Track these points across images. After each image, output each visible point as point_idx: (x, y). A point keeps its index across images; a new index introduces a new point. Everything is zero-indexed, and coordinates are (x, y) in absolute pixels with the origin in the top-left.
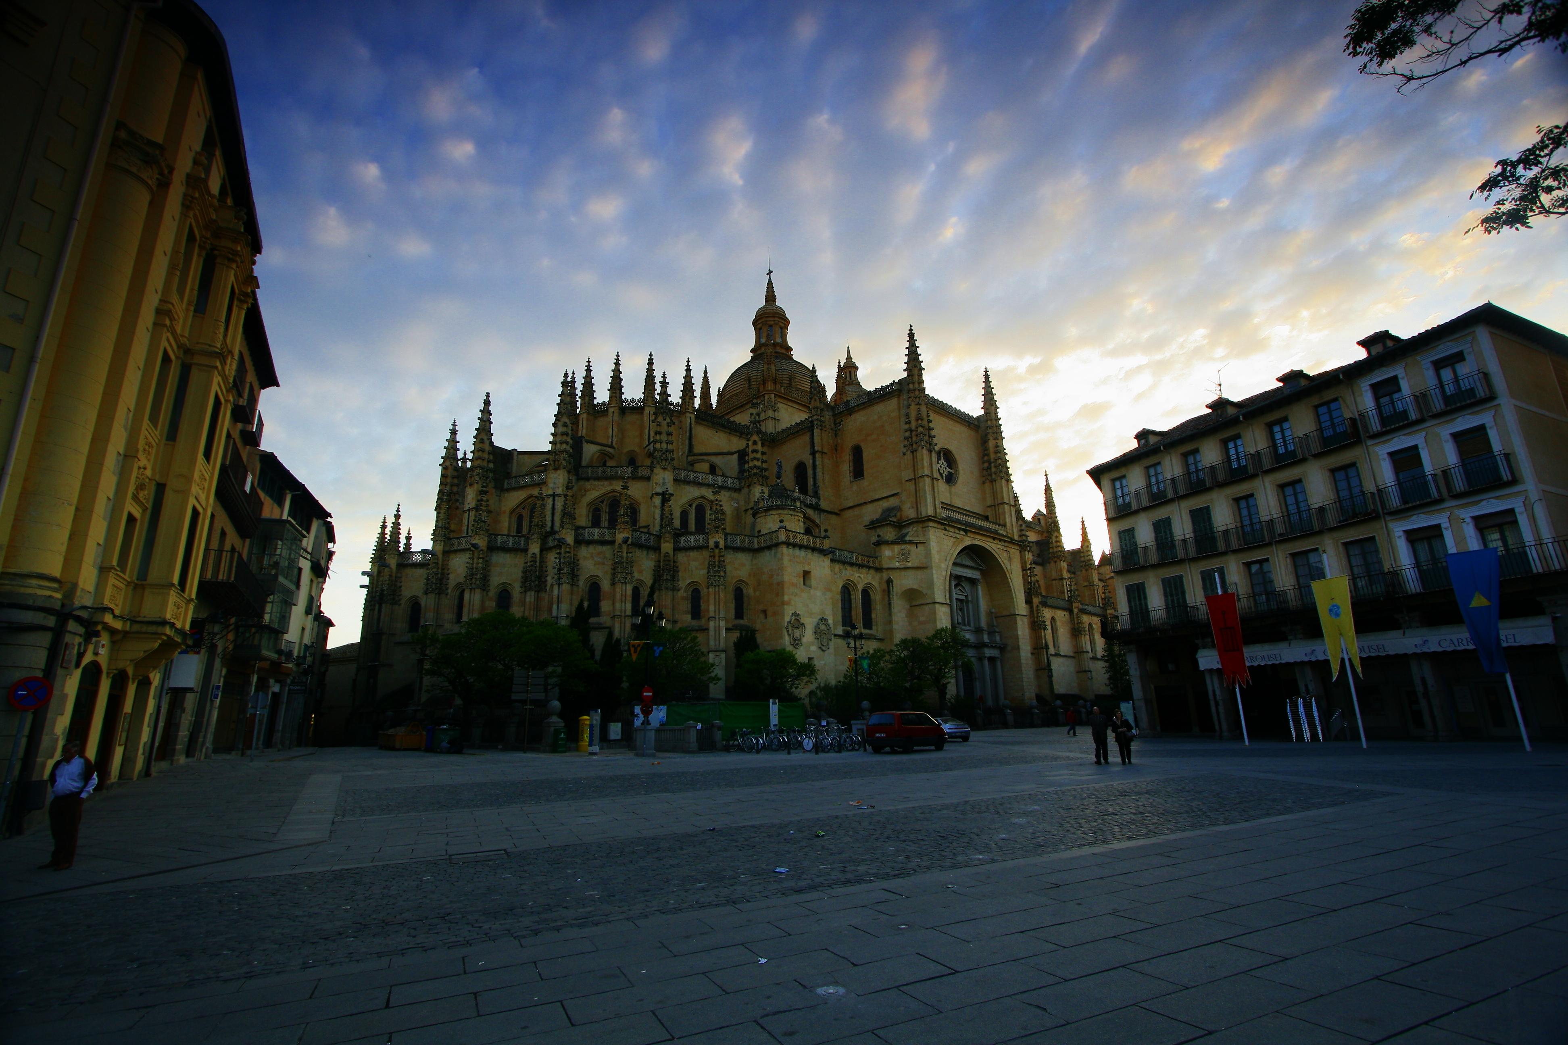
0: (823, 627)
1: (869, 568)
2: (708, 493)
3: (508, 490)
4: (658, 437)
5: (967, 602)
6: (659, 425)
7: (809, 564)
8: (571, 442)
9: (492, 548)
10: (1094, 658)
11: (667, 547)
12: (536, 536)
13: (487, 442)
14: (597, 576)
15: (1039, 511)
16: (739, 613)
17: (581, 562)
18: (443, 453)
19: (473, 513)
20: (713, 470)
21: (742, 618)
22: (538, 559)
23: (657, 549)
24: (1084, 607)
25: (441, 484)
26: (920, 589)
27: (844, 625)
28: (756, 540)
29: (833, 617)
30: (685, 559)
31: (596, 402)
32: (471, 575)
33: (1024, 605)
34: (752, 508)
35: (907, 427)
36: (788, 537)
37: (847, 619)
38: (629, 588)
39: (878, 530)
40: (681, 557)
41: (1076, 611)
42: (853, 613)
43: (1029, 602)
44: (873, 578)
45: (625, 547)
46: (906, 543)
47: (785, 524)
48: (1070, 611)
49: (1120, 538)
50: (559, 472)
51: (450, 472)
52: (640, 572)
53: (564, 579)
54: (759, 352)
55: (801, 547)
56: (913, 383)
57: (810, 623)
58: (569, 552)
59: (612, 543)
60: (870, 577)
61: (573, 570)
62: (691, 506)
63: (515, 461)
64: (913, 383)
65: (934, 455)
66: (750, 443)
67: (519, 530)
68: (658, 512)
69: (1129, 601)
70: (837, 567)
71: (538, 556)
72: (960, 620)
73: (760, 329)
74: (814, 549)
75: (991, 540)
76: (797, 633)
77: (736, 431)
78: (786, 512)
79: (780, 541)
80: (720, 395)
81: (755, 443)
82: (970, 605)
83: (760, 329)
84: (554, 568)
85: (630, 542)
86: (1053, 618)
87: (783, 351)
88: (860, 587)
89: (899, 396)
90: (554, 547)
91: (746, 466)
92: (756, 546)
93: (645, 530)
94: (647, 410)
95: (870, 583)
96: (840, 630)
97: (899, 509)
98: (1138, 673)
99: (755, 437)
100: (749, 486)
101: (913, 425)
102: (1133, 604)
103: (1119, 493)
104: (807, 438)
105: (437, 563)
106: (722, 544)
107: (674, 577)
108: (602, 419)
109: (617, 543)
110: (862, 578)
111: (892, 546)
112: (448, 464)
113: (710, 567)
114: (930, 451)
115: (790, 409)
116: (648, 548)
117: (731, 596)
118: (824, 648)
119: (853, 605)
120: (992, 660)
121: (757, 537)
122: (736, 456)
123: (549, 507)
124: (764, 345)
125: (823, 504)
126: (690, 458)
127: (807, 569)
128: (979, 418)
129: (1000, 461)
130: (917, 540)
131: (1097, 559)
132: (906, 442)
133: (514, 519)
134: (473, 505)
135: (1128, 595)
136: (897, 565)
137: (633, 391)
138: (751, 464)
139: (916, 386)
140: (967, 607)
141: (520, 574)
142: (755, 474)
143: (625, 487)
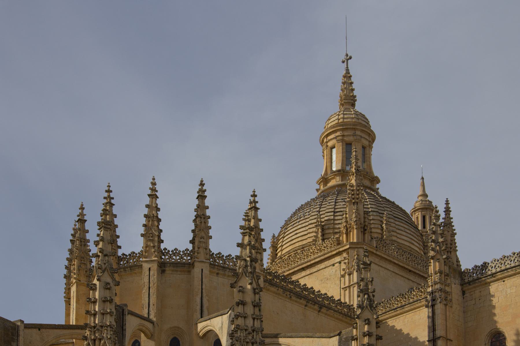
31: (120, 253)
54: (330, 184)
77: (315, 303)
87: (367, 183)
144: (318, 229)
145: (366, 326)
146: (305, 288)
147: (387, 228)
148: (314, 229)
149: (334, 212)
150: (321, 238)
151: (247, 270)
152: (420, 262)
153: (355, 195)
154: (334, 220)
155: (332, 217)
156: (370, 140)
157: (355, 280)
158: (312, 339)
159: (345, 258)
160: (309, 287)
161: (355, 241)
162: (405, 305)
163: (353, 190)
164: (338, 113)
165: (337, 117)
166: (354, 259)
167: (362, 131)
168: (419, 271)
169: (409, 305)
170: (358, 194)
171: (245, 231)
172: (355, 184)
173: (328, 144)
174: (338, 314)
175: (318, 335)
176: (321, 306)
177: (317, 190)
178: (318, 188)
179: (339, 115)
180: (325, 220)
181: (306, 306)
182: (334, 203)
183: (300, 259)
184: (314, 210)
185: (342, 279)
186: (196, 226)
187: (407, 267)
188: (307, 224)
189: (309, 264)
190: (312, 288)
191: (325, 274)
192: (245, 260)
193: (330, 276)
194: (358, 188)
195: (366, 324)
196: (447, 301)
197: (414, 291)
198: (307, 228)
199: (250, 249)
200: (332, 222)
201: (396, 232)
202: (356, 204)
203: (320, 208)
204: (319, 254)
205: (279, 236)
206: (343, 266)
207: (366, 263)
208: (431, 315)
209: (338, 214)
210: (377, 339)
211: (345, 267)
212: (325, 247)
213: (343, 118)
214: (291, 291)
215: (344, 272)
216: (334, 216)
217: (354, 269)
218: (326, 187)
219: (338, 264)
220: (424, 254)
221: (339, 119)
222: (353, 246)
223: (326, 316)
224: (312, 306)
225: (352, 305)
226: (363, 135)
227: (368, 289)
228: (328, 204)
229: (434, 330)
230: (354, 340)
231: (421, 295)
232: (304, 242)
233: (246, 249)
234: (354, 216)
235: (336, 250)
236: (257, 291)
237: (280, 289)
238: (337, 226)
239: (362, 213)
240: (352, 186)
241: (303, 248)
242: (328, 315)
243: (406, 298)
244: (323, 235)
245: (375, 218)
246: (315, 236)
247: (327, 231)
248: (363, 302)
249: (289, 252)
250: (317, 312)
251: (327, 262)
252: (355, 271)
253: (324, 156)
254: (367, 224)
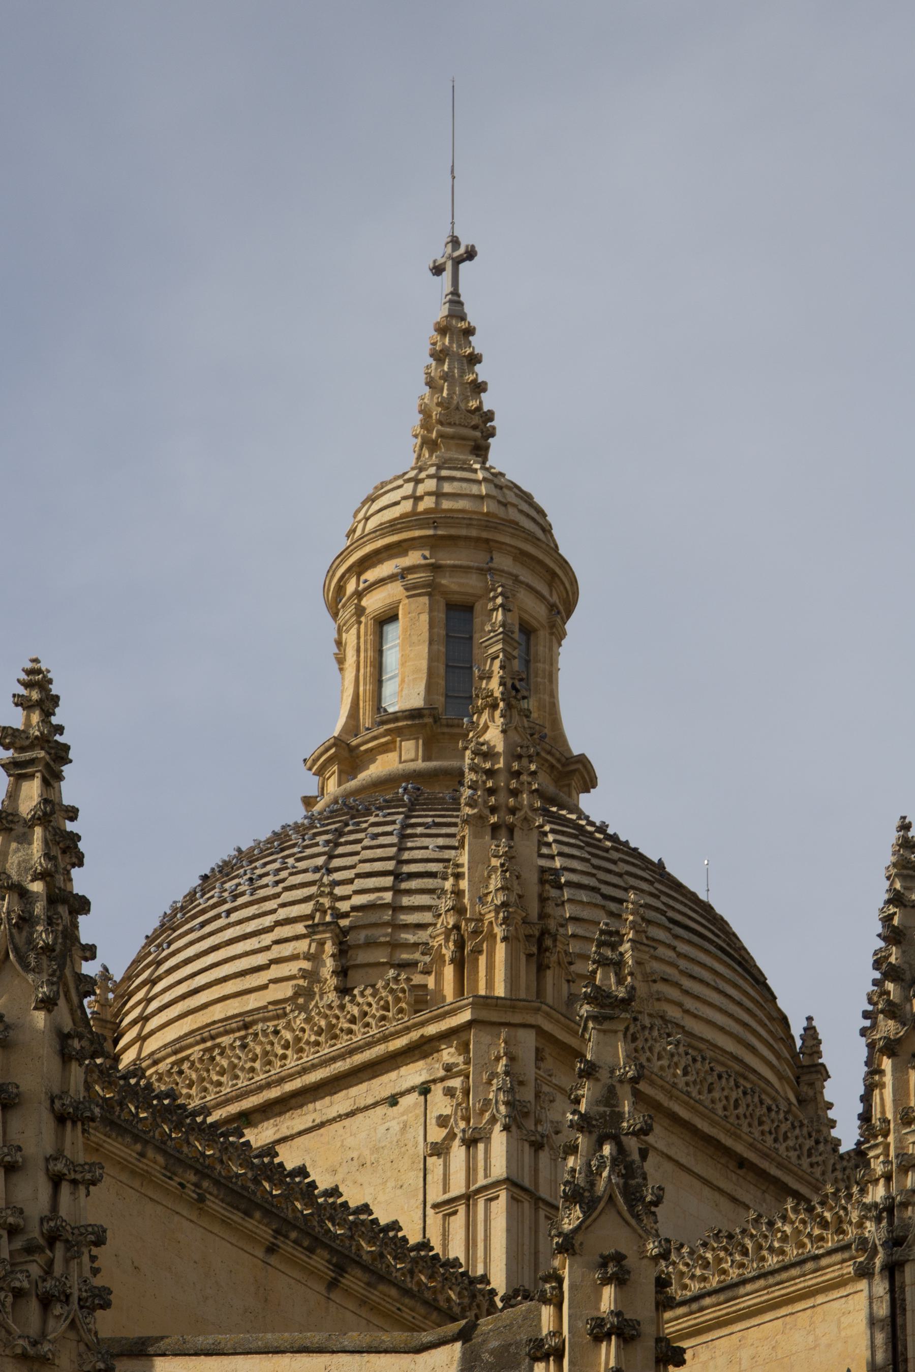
144: (322, 944)
145: (608, 1294)
146: (266, 1165)
147: (638, 963)
148: (302, 946)
149: (398, 876)
150: (332, 982)
151: (30, 941)
152: (784, 1127)
153: (502, 795)
154: (397, 908)
155: (388, 897)
156: (555, 599)
157: (499, 1169)
158: (325, 1359)
159: (448, 1068)
160: (289, 1166)
161: (500, 990)
162: (744, 1282)
163: (490, 773)
164: (412, 474)
165: (408, 488)
166: (494, 1075)
167: (522, 556)
168: (780, 1166)
169: (761, 1283)
170: (515, 793)
171: (27, 755)
172: (500, 748)
173: (364, 603)
174: (422, 1310)
175: (354, 1338)
176: (343, 1261)
177: (308, 802)
178: (314, 792)
179: (417, 481)
180: (354, 908)
181: (271, 1250)
182: (394, 839)
183: (232, 1071)
184: (302, 865)
185: (435, 1163)
187: (728, 1142)
188: (268, 921)
189: (274, 1093)
190: (302, 1171)
191: (350, 1141)
192: (23, 893)
193: (376, 1150)
194: (515, 766)
195: (606, 1281)
197: (784, 1218)
198: (267, 939)
199: (46, 842)
200: (387, 916)
201: (677, 985)
202: (504, 832)
203: (331, 857)
204: (325, 1050)
205: (129, 977)
206: (440, 1104)
207: (609, 995)
208: (883, 1310)
209: (414, 884)
210: (658, 1361)
211: (447, 1111)
212: (353, 1020)
213: (438, 495)
215: (444, 1132)
216: (398, 892)
217: (493, 1120)
218: (353, 784)
219: (414, 1097)
220: (800, 1102)
221: (417, 499)
222: (490, 1015)
223: (363, 1312)
224: (299, 1254)
225: (485, 1279)
226: (526, 576)
227: (620, 1116)
228: (367, 842)
230: (545, 1358)
231: (821, 1238)
232: (253, 1002)
233: (25, 839)
234: (495, 882)
235: (408, 1029)
236: (76, 1044)
237: (150, 1153)
238: (410, 937)
240: (489, 754)
241: (246, 1026)
242: (374, 1308)
243: (745, 1253)
244: (342, 972)
245: (585, 914)
246: (304, 974)
247: (362, 957)
248: (592, 1175)
249: (177, 1046)
250: (322, 1288)
251: (363, 1087)
252: (498, 1127)
253: (341, 661)
254: (552, 925)
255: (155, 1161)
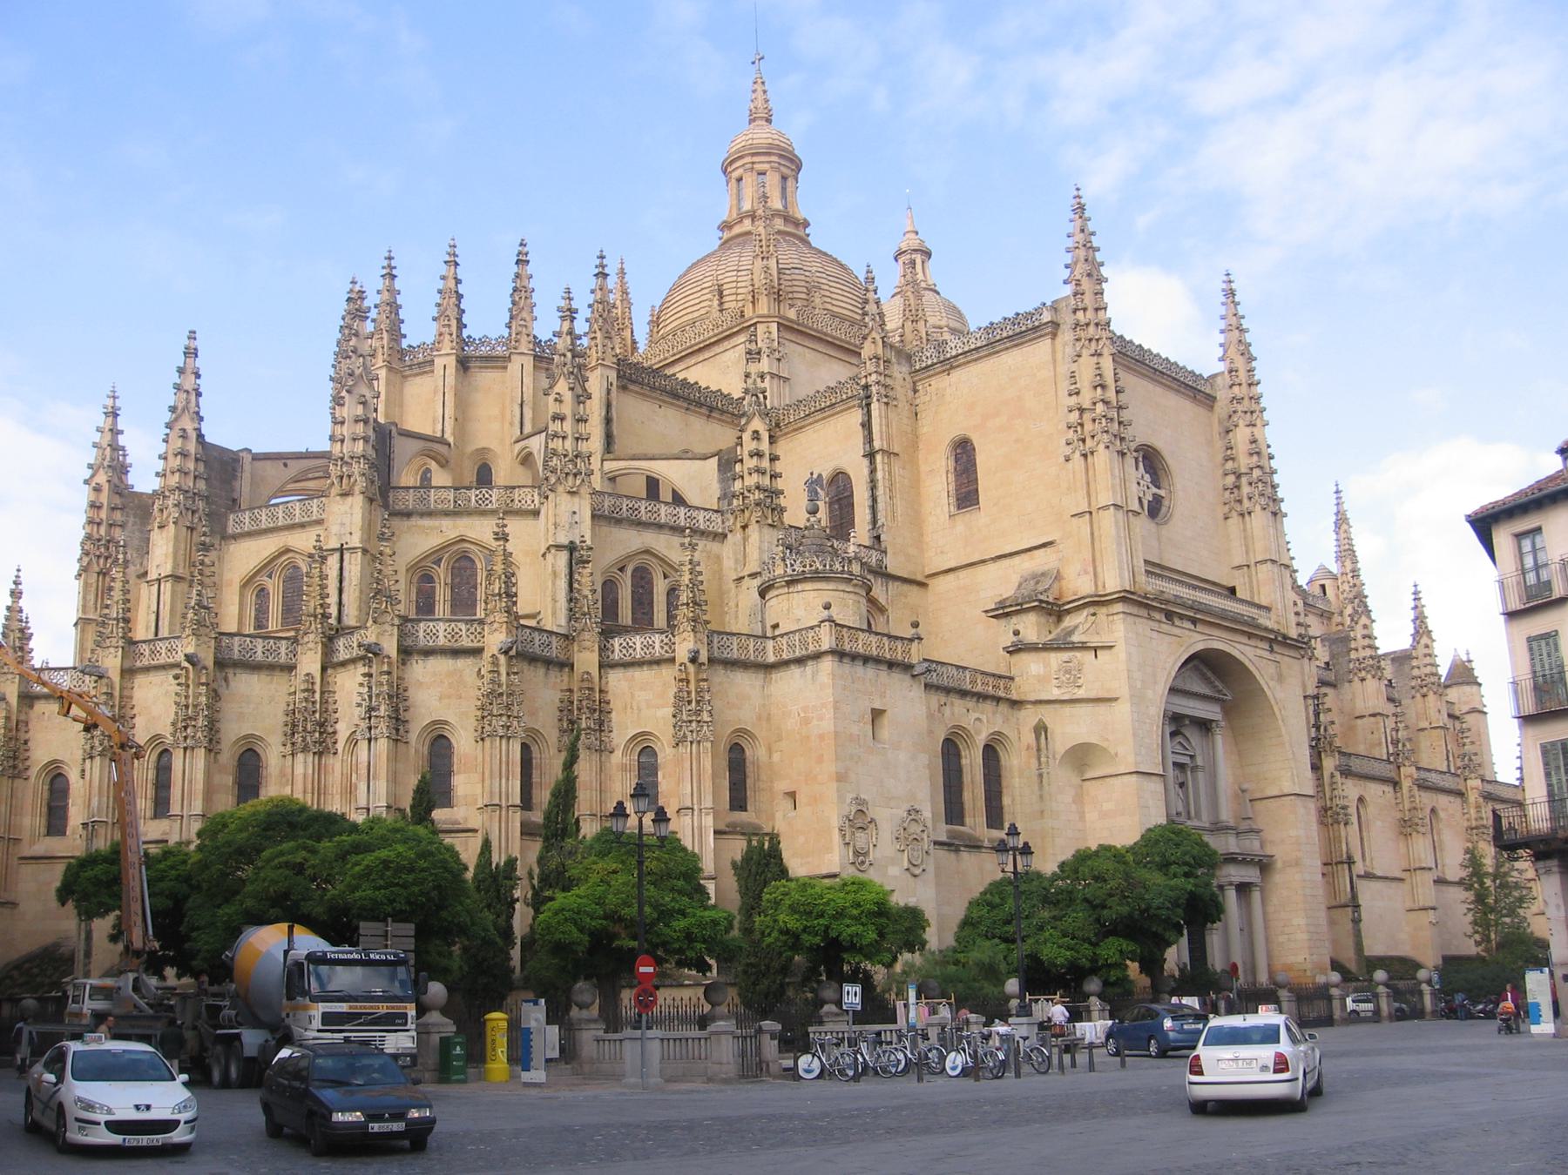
0: (915, 829)
1: (998, 700)
2: (669, 547)
3: (235, 537)
4: (555, 427)
5: (1195, 769)
6: (559, 400)
7: (883, 695)
8: (371, 433)
9: (220, 664)
10: (1440, 881)
11: (586, 659)
12: (312, 636)
13: (193, 435)
14: (446, 722)
15: (1322, 568)
16: (738, 800)
17: (410, 693)
18: (91, 456)
19: (167, 587)
20: (653, 485)
21: (743, 808)
22: (317, 687)
23: (566, 665)
24: (1424, 775)
25: (90, 522)
26: (1105, 744)
27: (949, 821)
28: (770, 644)
29: (929, 804)
30: (624, 684)
31: (405, 344)
32: (184, 723)
33: (1309, 773)
34: (753, 575)
35: (1073, 401)
36: (839, 639)
37: (954, 811)
38: (516, 748)
39: (1014, 619)
40: (617, 681)
41: (1406, 784)
42: (967, 796)
43: (1316, 768)
44: (1006, 720)
45: (502, 659)
46: (1074, 647)
47: (834, 612)
48: (1396, 784)
49: (1531, 649)
50: (350, 499)
51: (104, 498)
52: (533, 713)
53: (383, 727)
54: (737, 230)
55: (866, 659)
56: (1085, 310)
57: (887, 818)
58: (389, 673)
59: (477, 652)
60: (999, 719)
61: (397, 710)
62: (621, 569)
63: (247, 475)
64: (1085, 310)
65: (1130, 460)
66: (747, 436)
67: (260, 623)
68: (563, 583)
69: (1548, 775)
70: (936, 699)
71: (318, 680)
72: (1181, 809)
73: (739, 180)
74: (891, 665)
75: (1244, 639)
76: (861, 839)
77: (701, 405)
78: (832, 586)
79: (825, 646)
80: (655, 322)
81: (756, 436)
82: (1200, 775)
83: (739, 180)
84: (359, 705)
85: (513, 653)
86: (1361, 800)
88: (981, 739)
89: (1054, 336)
90: (353, 661)
91: (738, 485)
92: (771, 659)
93: (532, 623)
94: (517, 361)
95: (999, 733)
96: (943, 832)
97: (1058, 577)
98: (1562, 913)
99: (757, 424)
100: (744, 527)
101: (1086, 399)
102: (1554, 781)
103: (1529, 562)
104: (857, 416)
105: (110, 695)
106: (703, 657)
107: (601, 724)
108: (418, 380)
109: (487, 655)
110: (982, 723)
111: (1044, 655)
112: (102, 478)
113: (681, 700)
114: (1122, 454)
115: (809, 355)
116: (548, 663)
117: (724, 763)
118: (917, 871)
119: (967, 778)
120: (1243, 889)
121: (774, 638)
122: (714, 461)
123: (333, 573)
124: (753, 216)
125: (893, 564)
126: (609, 466)
127: (877, 706)
128: (1214, 376)
129: (1256, 473)
130: (1094, 640)
131: (1443, 671)
132: (1070, 434)
133: (250, 598)
134: (167, 569)
135: (1546, 764)
136: (1056, 693)
137: (487, 320)
138: (751, 481)
139: (1090, 314)
140: (1195, 780)
141: (282, 718)
142: (757, 505)
143: (502, 537)
161: (766, 312)
176: (711, 409)
186: (514, 303)
196: (889, 401)
214: (664, 391)
229: (871, 441)
239: (775, 273)
255: (646, 390)
